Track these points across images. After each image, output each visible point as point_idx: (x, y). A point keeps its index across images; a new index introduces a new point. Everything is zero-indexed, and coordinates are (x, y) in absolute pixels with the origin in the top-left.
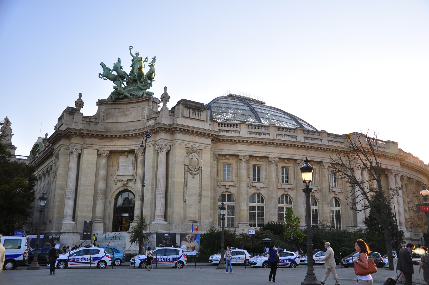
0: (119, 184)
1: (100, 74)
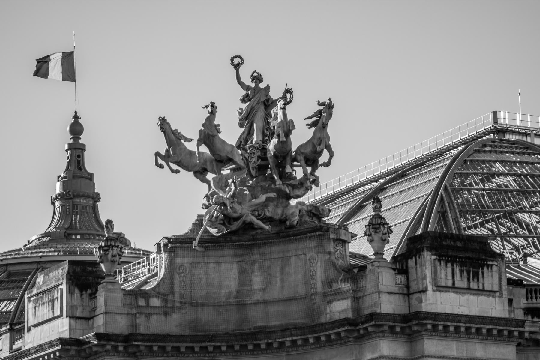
1: (157, 154)
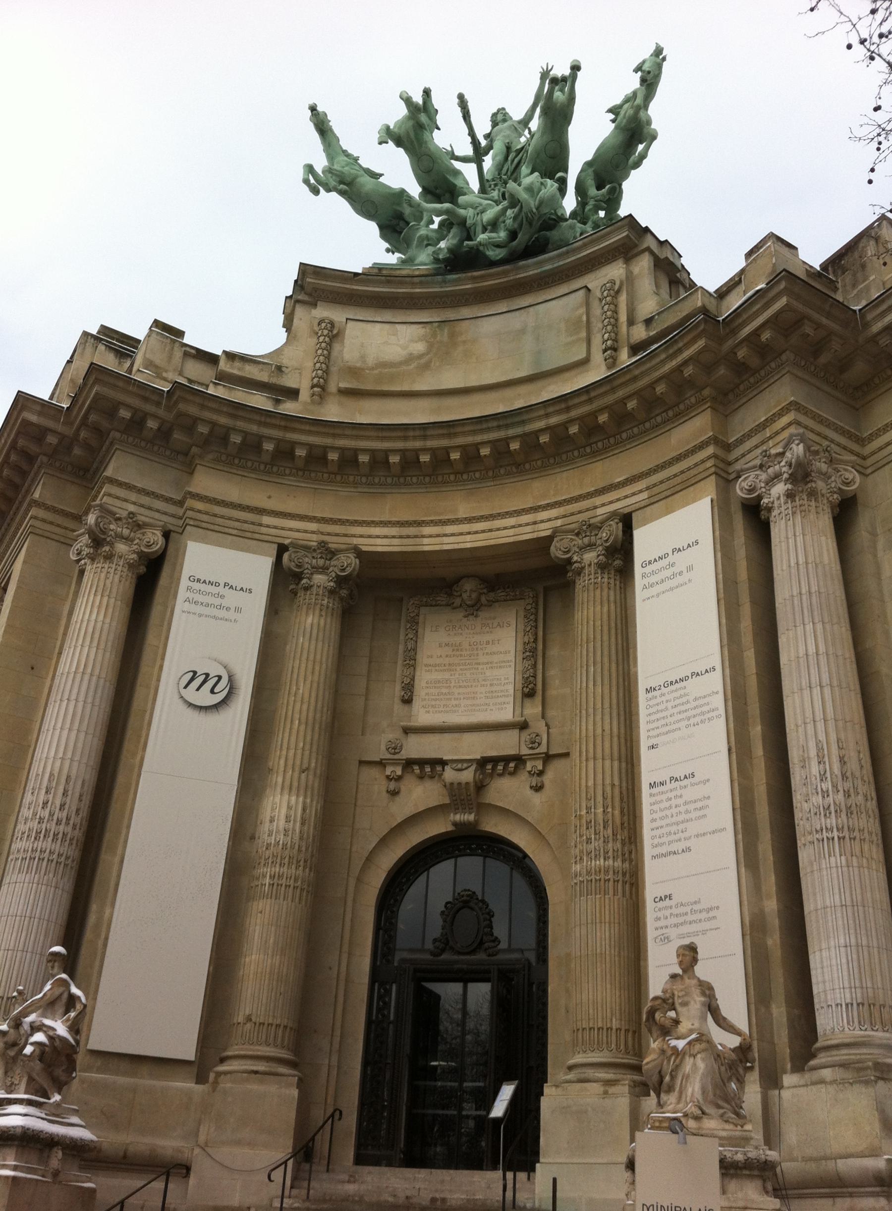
0: (420, 795)
1: (310, 169)
